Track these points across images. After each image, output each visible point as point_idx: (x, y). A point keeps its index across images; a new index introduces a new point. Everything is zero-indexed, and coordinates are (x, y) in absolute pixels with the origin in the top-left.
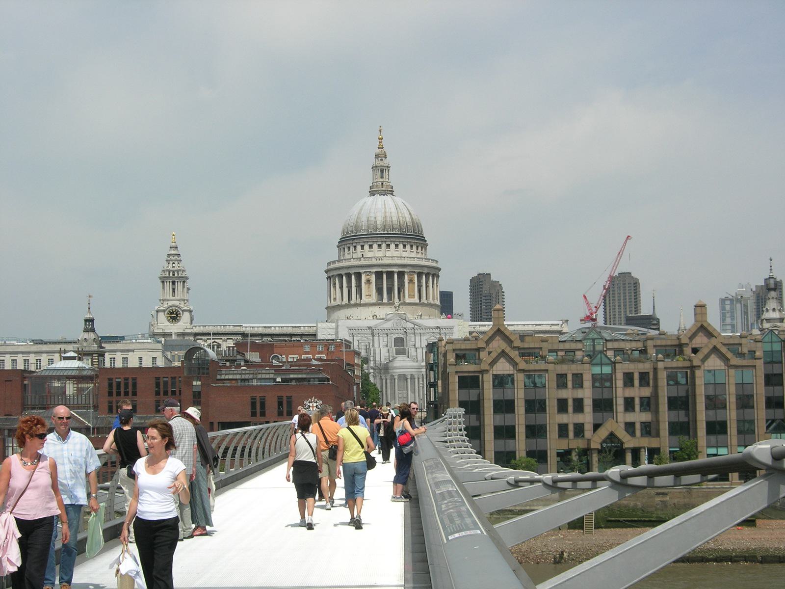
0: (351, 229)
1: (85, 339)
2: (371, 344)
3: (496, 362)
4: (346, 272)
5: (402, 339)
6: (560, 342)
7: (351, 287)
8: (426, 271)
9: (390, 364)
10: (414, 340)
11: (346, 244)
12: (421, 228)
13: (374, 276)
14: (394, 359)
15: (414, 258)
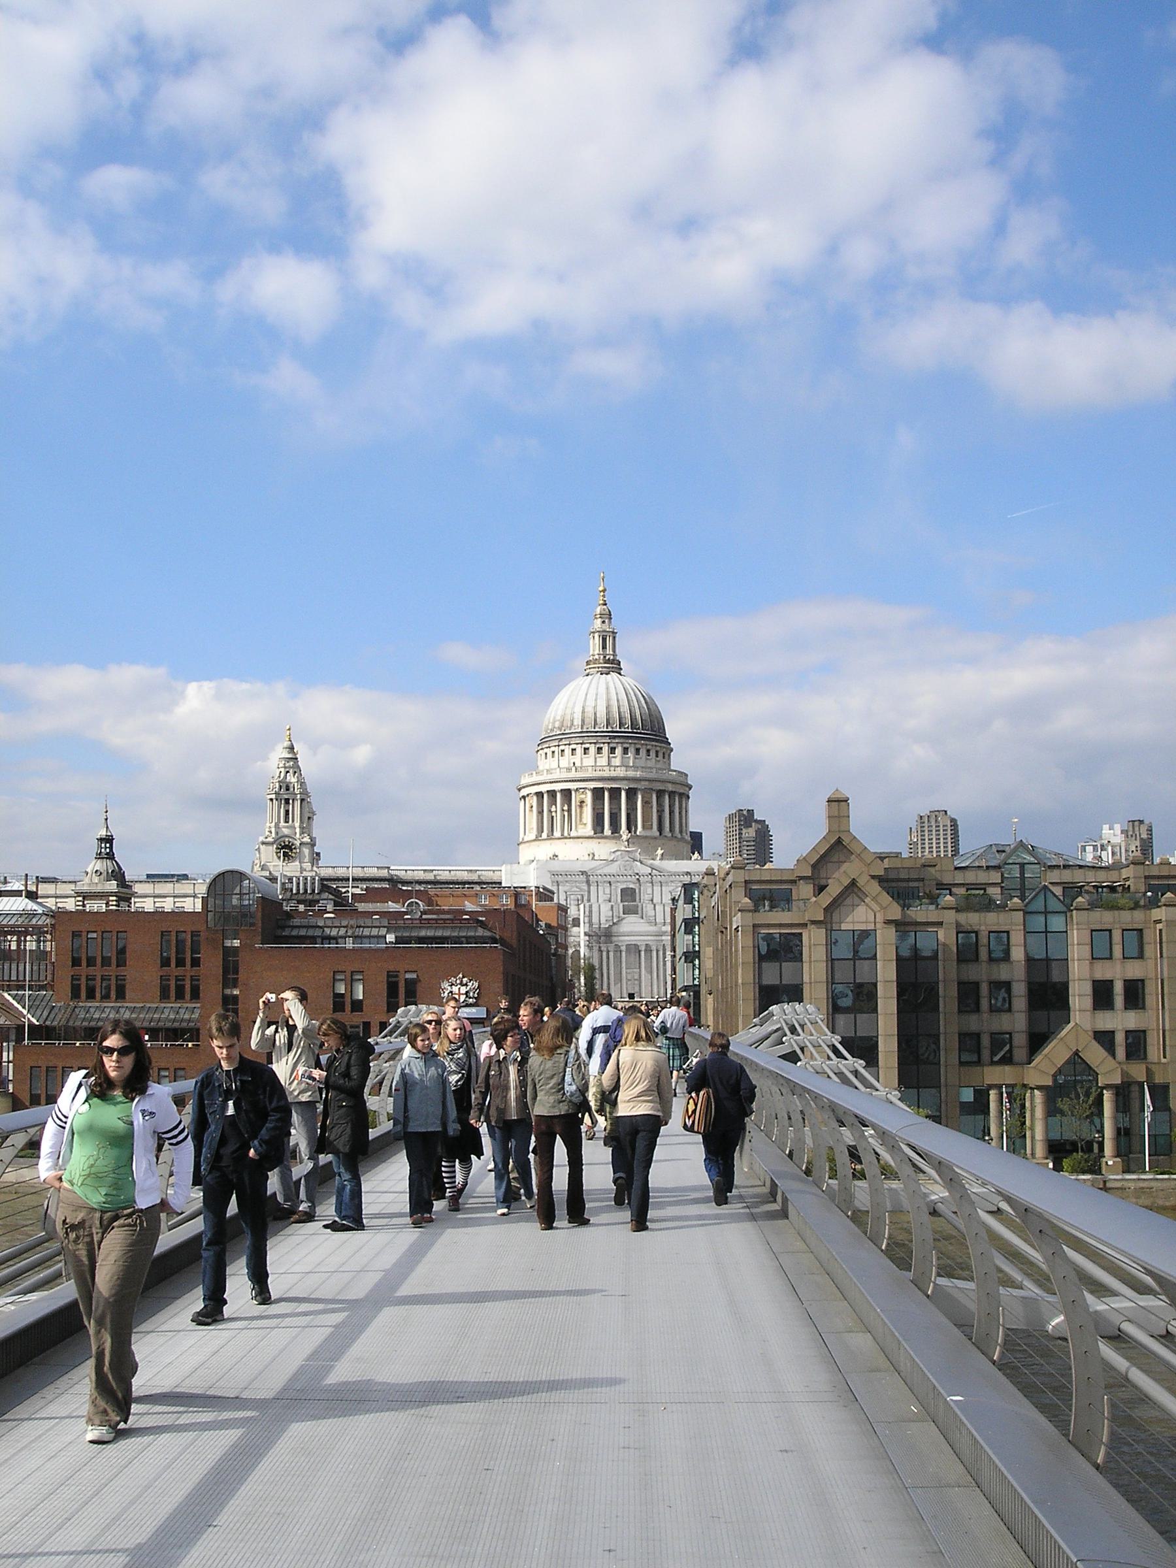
0: (557, 724)
1: (96, 871)
2: (586, 898)
3: (839, 905)
4: (549, 789)
5: (633, 890)
6: (956, 868)
7: (556, 812)
8: (670, 787)
9: (615, 929)
10: (651, 892)
11: (550, 747)
12: (663, 724)
13: (589, 794)
14: (621, 920)
15: (650, 768)
